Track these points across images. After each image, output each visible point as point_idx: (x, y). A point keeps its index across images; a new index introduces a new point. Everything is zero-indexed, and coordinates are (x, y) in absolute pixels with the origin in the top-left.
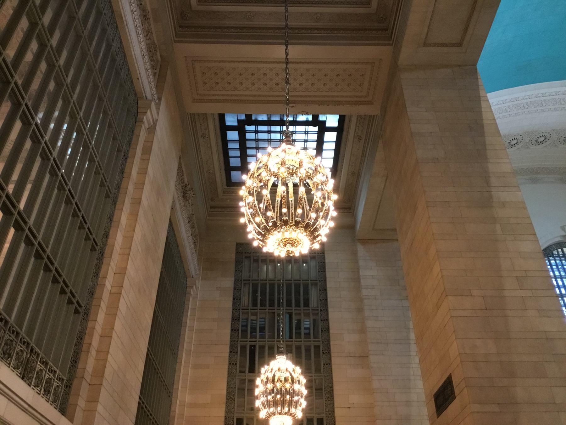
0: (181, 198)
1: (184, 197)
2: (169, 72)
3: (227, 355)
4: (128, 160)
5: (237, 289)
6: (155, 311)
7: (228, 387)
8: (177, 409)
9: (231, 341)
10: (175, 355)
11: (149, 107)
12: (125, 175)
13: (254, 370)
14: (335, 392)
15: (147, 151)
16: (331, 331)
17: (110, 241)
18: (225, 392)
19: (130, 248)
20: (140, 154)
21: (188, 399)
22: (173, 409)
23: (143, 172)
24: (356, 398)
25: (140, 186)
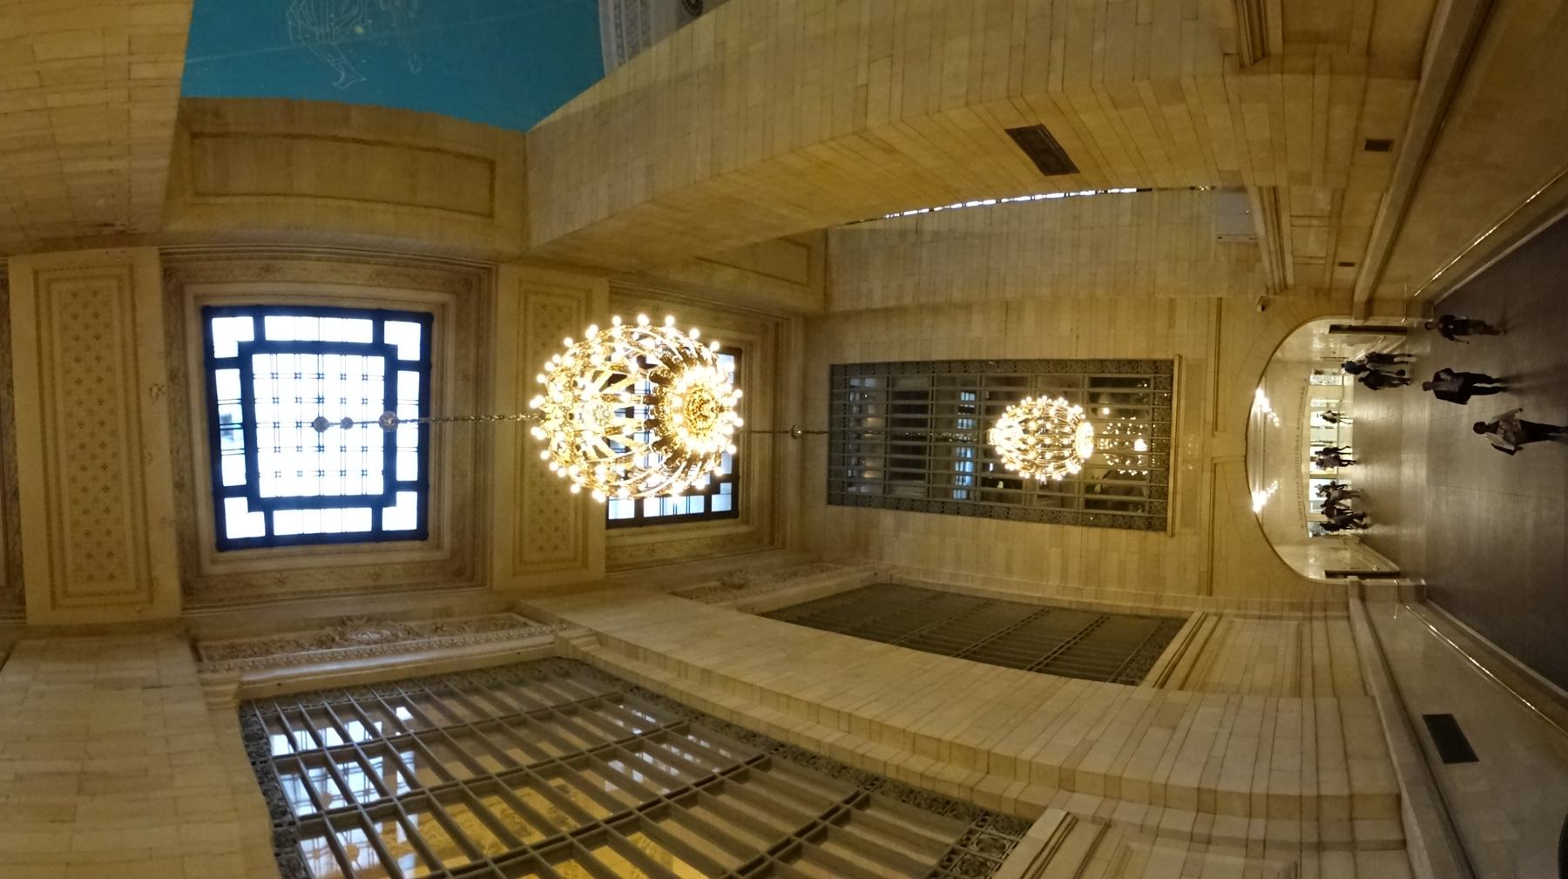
0: (742, 592)
1: (740, 587)
2: (531, 603)
3: (994, 522)
4: (642, 684)
5: (898, 505)
6: (901, 645)
7: (1041, 521)
8: (1067, 599)
9: (974, 515)
10: (989, 602)
11: (566, 641)
12: (662, 693)
13: (1014, 483)
14: (1055, 357)
15: (633, 651)
16: (967, 357)
17: (762, 730)
18: (1047, 526)
19: (778, 694)
20: (636, 663)
21: (1054, 582)
22: (1066, 605)
23: (662, 660)
24: (1065, 325)
25: (683, 669)
